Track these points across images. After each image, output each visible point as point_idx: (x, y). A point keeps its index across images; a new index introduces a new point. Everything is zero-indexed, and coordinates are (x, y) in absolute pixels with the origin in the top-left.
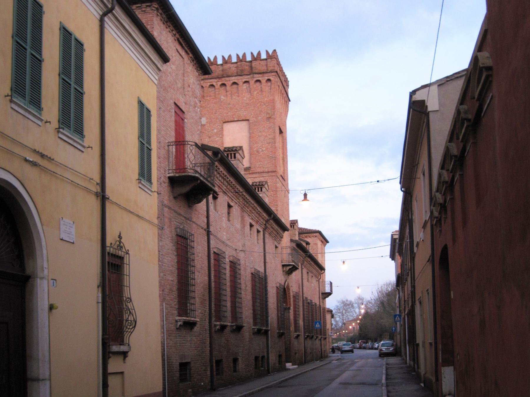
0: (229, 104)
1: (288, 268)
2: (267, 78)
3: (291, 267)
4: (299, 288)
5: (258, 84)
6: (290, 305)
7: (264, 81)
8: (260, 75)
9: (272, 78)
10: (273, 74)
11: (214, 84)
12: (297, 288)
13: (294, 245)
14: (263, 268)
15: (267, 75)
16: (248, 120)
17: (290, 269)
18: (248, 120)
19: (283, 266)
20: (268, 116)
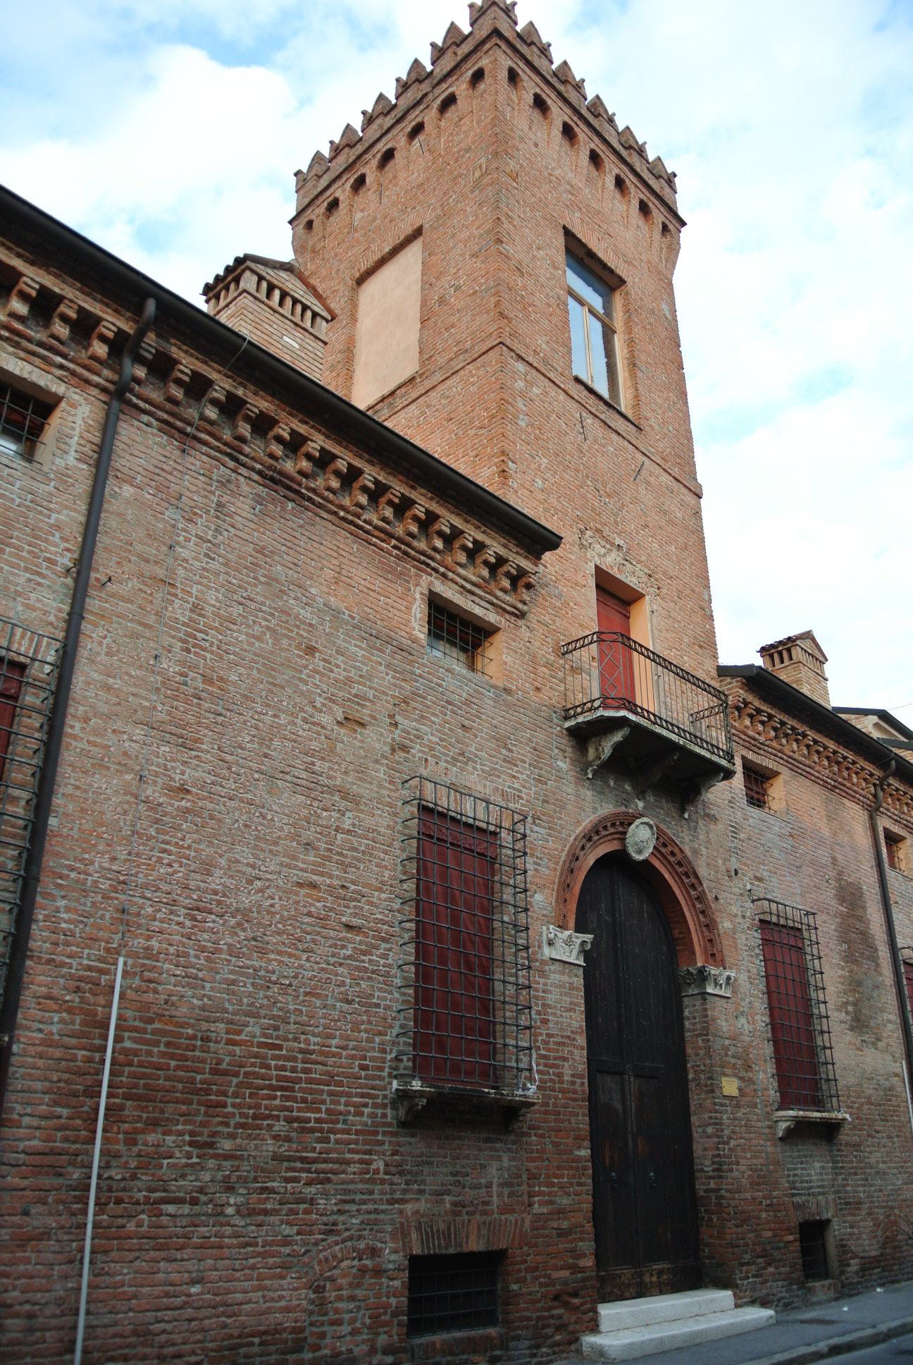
0: (375, 219)
1: (607, 746)
2: (470, 73)
3: (618, 737)
4: (850, 897)
5: (452, 113)
6: (715, 957)
7: (465, 86)
8: (450, 80)
9: (484, 62)
10: (488, 46)
11: (337, 195)
12: (828, 897)
13: (736, 691)
14: (50, 603)
15: (470, 63)
16: (418, 232)
17: (617, 748)
18: (418, 232)
19: (582, 736)
20: (477, 174)
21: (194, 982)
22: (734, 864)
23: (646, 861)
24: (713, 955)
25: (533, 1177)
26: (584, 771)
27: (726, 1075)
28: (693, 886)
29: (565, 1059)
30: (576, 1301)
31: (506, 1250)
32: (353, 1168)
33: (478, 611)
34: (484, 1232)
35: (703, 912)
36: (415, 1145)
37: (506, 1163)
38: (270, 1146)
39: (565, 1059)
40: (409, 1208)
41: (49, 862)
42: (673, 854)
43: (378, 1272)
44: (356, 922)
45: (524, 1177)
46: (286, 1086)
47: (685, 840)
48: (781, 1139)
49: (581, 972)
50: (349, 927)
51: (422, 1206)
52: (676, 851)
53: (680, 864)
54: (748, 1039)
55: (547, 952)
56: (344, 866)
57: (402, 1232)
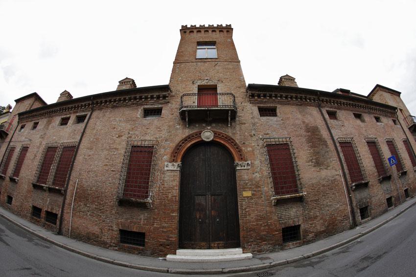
21: (87, 182)
22: (253, 132)
23: (213, 140)
24: (242, 159)
25: (154, 218)
26: (186, 126)
27: (245, 191)
28: (232, 142)
29: (169, 193)
30: (168, 247)
31: (145, 233)
32: (109, 212)
33: (156, 106)
34: (138, 228)
35: (237, 148)
36: (122, 209)
37: (146, 215)
38: (94, 206)
39: (169, 193)
40: (120, 220)
41: (74, 168)
42: (222, 136)
43: (112, 230)
44: (114, 170)
45: (152, 218)
46: (98, 197)
47: (229, 132)
48: (274, 205)
49: (178, 172)
50: (112, 171)
51: (122, 220)
52: (224, 135)
53: (226, 138)
54: (258, 179)
55: (166, 169)
56: (113, 161)
57: (118, 224)
